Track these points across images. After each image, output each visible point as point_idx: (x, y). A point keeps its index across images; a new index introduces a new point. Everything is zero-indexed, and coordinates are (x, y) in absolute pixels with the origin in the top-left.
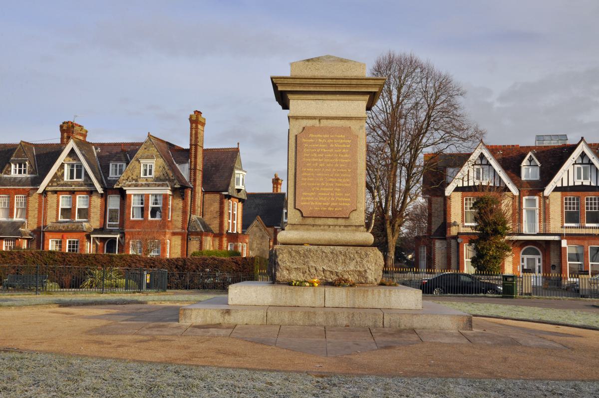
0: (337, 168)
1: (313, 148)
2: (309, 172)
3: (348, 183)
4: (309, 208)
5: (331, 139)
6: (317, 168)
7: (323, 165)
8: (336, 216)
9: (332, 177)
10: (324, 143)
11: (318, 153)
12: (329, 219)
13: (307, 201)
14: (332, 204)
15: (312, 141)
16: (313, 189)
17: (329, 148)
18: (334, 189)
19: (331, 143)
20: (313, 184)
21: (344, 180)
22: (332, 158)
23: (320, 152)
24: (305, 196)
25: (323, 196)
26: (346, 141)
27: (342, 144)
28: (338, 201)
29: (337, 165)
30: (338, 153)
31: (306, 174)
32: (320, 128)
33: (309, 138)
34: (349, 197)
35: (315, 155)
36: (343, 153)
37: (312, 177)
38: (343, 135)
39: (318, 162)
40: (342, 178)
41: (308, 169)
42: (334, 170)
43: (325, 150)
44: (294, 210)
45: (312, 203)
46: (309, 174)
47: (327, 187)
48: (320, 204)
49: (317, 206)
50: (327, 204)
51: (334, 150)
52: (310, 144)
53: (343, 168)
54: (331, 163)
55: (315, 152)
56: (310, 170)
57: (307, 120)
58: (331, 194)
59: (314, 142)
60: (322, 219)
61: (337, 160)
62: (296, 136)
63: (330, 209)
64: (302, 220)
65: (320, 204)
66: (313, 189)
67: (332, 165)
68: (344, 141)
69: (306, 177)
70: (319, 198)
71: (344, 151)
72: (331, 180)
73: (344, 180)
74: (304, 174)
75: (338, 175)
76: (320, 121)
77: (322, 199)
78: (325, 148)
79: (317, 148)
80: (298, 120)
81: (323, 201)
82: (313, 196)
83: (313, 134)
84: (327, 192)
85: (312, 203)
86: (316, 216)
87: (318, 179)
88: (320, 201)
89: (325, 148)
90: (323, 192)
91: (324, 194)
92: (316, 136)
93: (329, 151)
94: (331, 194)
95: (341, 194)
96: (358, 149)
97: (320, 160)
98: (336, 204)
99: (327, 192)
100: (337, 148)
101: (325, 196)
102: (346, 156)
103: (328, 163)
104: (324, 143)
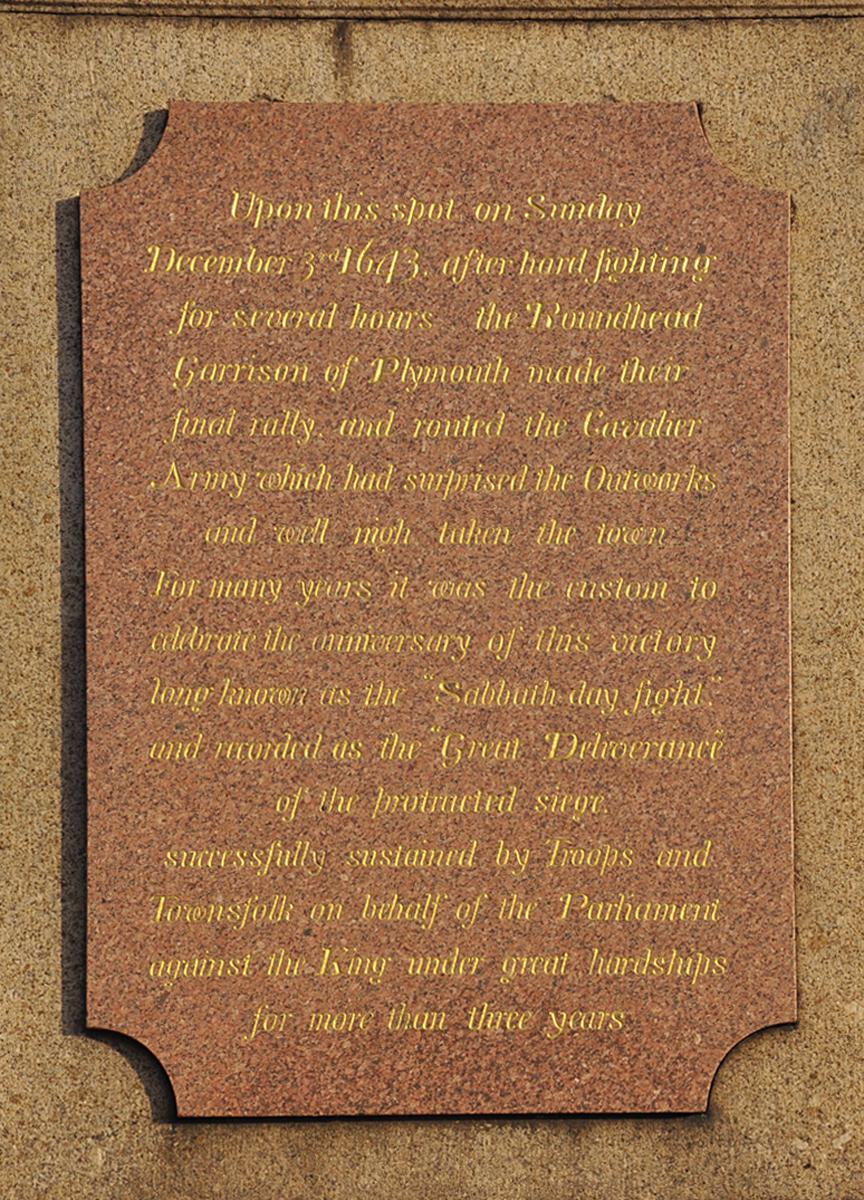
0: (550, 564)
1: (270, 351)
2: (231, 614)
3: (691, 727)
4: (246, 1017)
5: (487, 240)
6: (325, 566)
7: (400, 533)
8: (557, 1100)
9: (498, 670)
10: (402, 294)
11: (331, 406)
12: (485, 1137)
13: (223, 939)
14: (509, 969)
15: (265, 266)
16: (288, 808)
17: (467, 345)
18: (526, 802)
19: (482, 285)
20: (288, 749)
21: (644, 699)
22: (497, 456)
23: (359, 398)
24: (197, 887)
25: (408, 884)
26: (657, 265)
27: (609, 296)
28: (578, 937)
29: (555, 535)
30: (563, 403)
31: (194, 639)
32: (352, 119)
33: (230, 240)
34: (703, 884)
35: (301, 424)
36: (623, 402)
37: (269, 667)
38: (626, 194)
39: (341, 505)
40: (625, 674)
41: (219, 588)
42: (525, 588)
43: (410, 374)
44: (70, 1051)
45: (282, 965)
46: (239, 641)
47: (448, 780)
48: (374, 966)
49: (335, 993)
50: (457, 966)
51: (518, 372)
52: (244, 304)
53: (637, 564)
54: (491, 511)
55: (295, 392)
56: (248, 588)
57: (191, 35)
58: (502, 857)
59: (283, 284)
60: (400, 1137)
61: (552, 481)
62: (70, 214)
63: (488, 1020)
64: (168, 1153)
65: (374, 966)
66: (288, 808)
67: (504, 535)
68: (633, 263)
69: (201, 670)
70: (354, 906)
71: (635, 371)
72: (490, 694)
73: (644, 699)
74: (176, 640)
75: (567, 643)
76: (341, 40)
77: (394, 909)
78: (411, 345)
79: (323, 345)
80: (78, 37)
81: (400, 940)
82: (284, 881)
83: (272, 184)
84: (446, 832)
85: (282, 965)
86: (330, 1100)
87: (336, 695)
88: (369, 939)
89: (411, 345)
90: (400, 830)
91: (419, 858)
92: (305, 211)
93: (457, 374)
94: (502, 857)
95: (608, 856)
96: (798, 347)
97: (358, 482)
98: (554, 966)
99: (446, 832)
100: (554, 347)
101: (432, 880)
102: (661, 425)
103: (456, 510)
104: (402, 294)
